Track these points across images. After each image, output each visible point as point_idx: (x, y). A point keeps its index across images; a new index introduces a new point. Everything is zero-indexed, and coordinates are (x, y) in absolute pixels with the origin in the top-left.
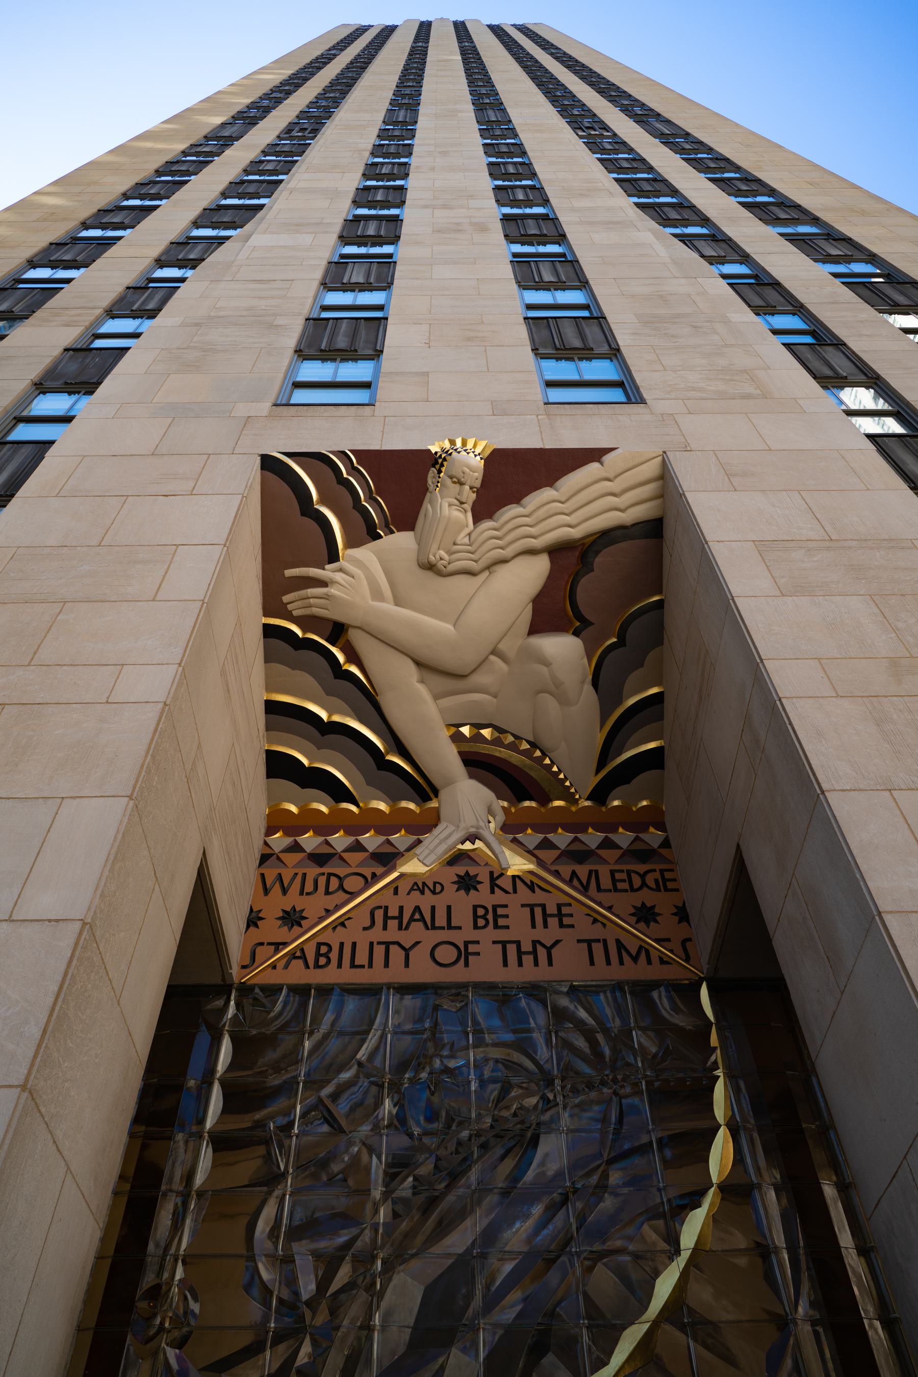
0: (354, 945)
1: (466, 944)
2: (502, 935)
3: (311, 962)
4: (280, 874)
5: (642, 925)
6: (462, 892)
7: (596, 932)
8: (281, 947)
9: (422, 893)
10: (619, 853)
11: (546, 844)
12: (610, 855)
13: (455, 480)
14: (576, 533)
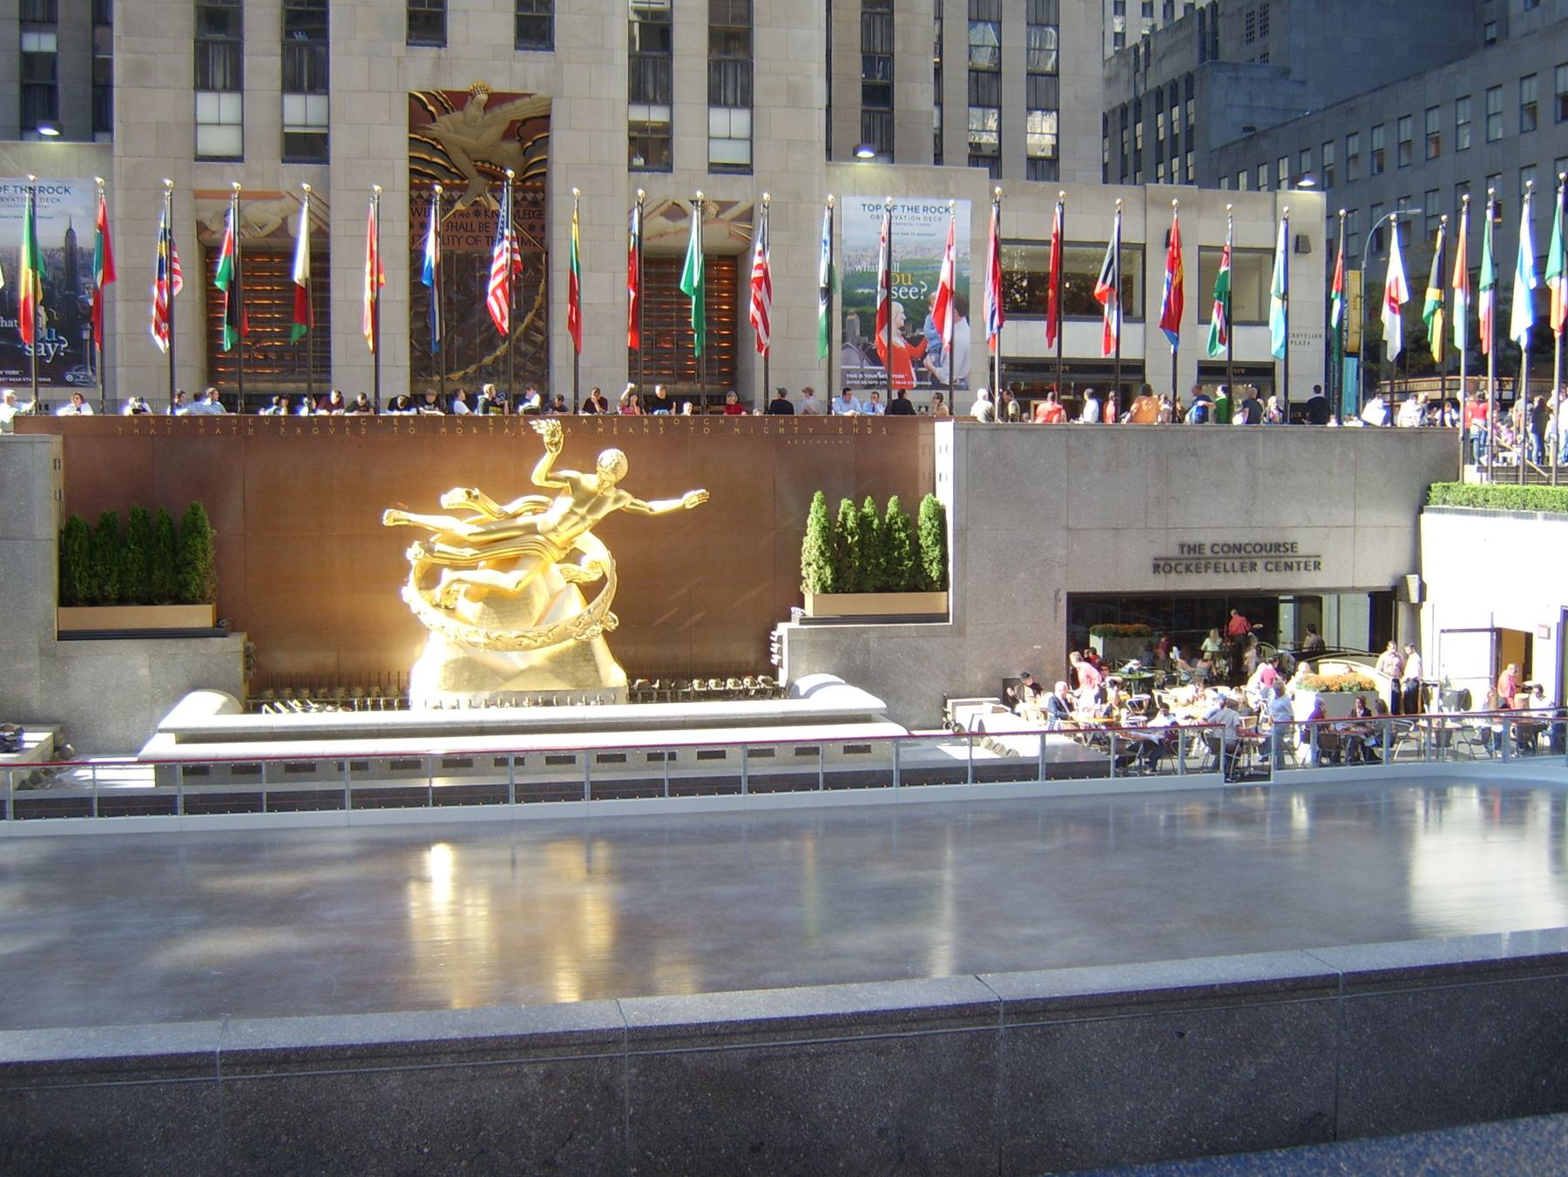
12: (524, 203)
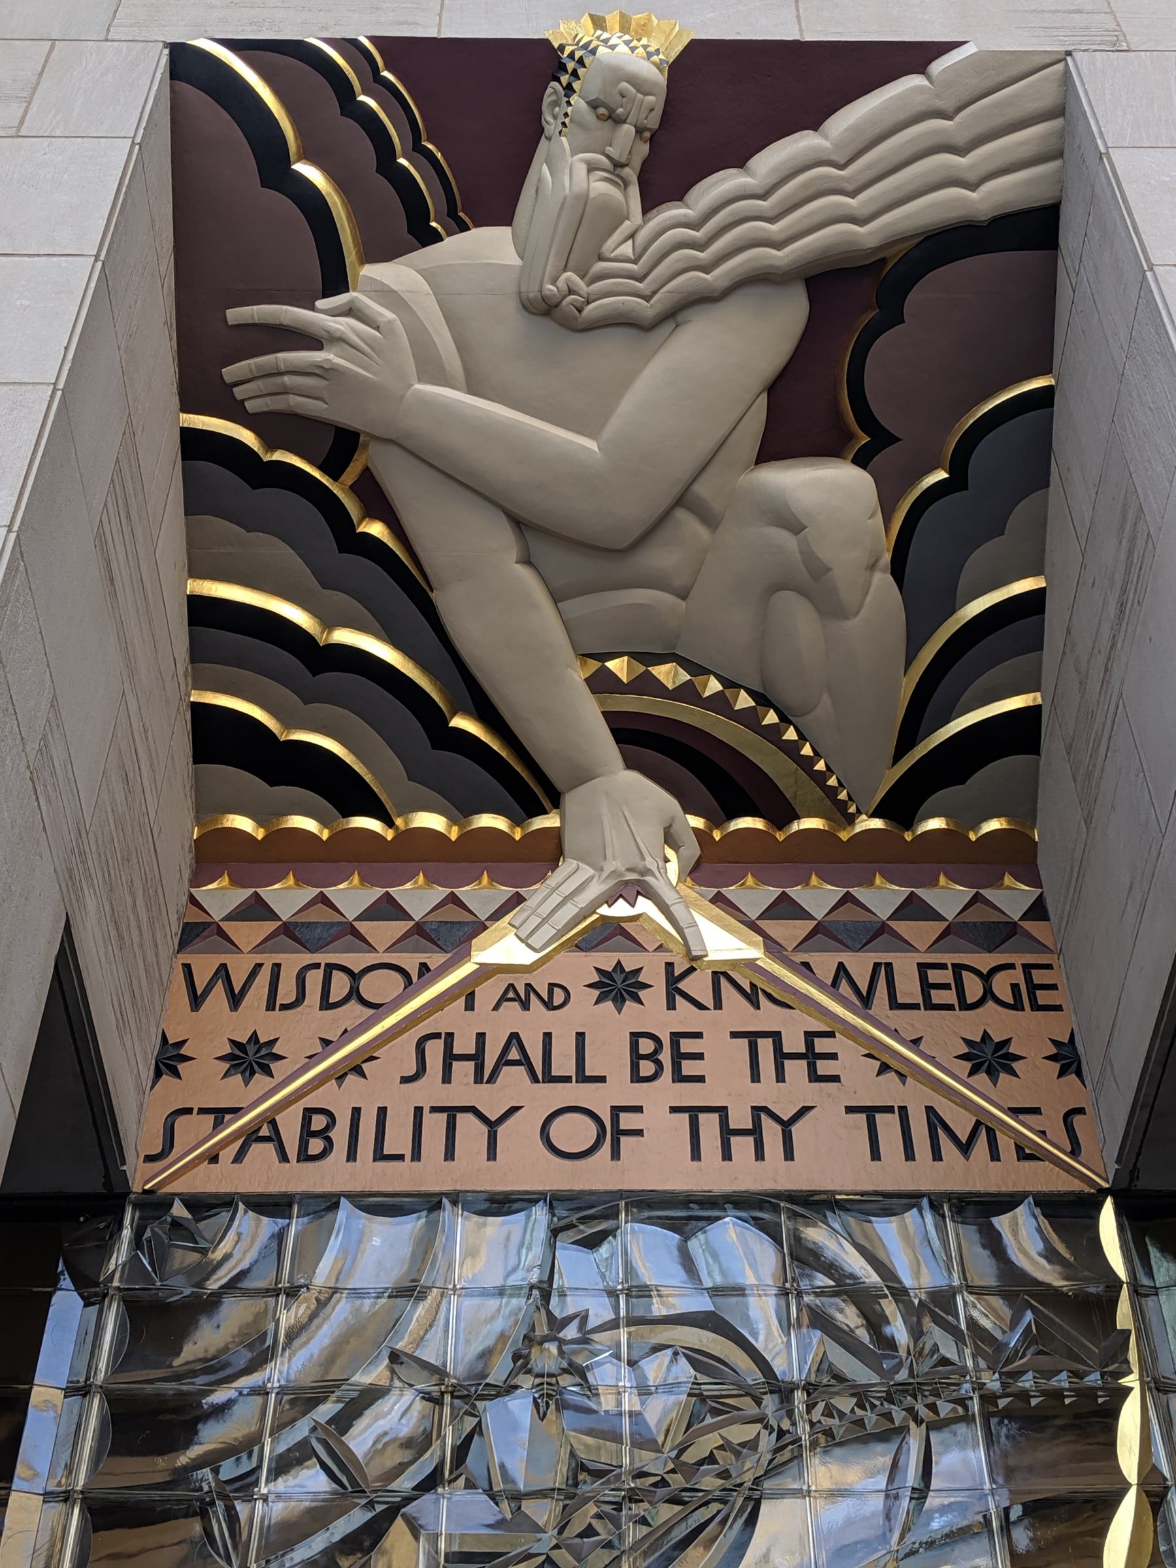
0: (382, 1111)
1: (616, 1111)
2: (691, 1095)
3: (292, 1150)
4: (224, 966)
5: (982, 1078)
6: (609, 1005)
7: (888, 1091)
8: (227, 1117)
9: (525, 1006)
10: (938, 927)
11: (784, 908)
12: (920, 933)
13: (602, 110)
14: (868, 235)
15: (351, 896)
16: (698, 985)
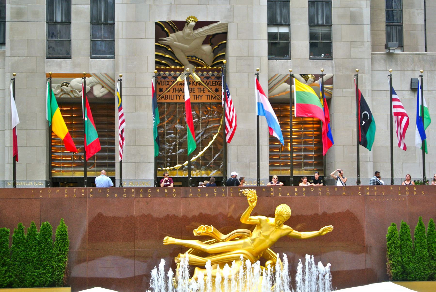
2: (194, 94)
7: (209, 93)
12: (213, 77)
15: (167, 73)
16: (195, 83)
